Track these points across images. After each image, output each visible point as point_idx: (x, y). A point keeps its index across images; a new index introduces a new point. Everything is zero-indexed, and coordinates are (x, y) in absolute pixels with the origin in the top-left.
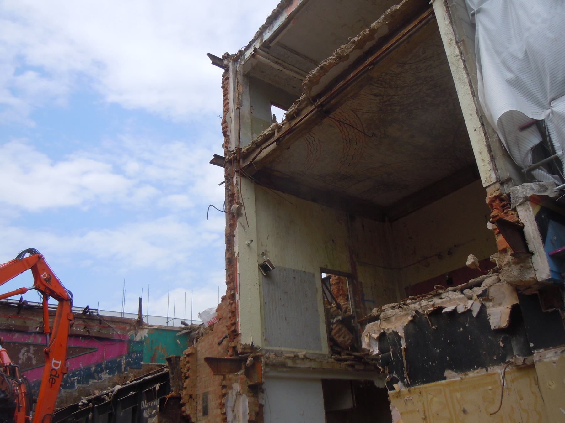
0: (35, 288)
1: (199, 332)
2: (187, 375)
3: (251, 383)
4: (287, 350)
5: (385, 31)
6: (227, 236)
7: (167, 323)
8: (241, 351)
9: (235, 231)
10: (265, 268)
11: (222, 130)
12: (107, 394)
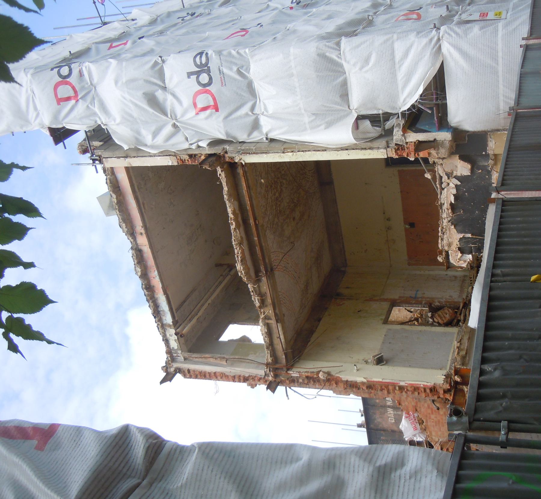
5: (236, 203)
8: (448, 385)
9: (343, 379)
10: (380, 361)
11: (240, 382)
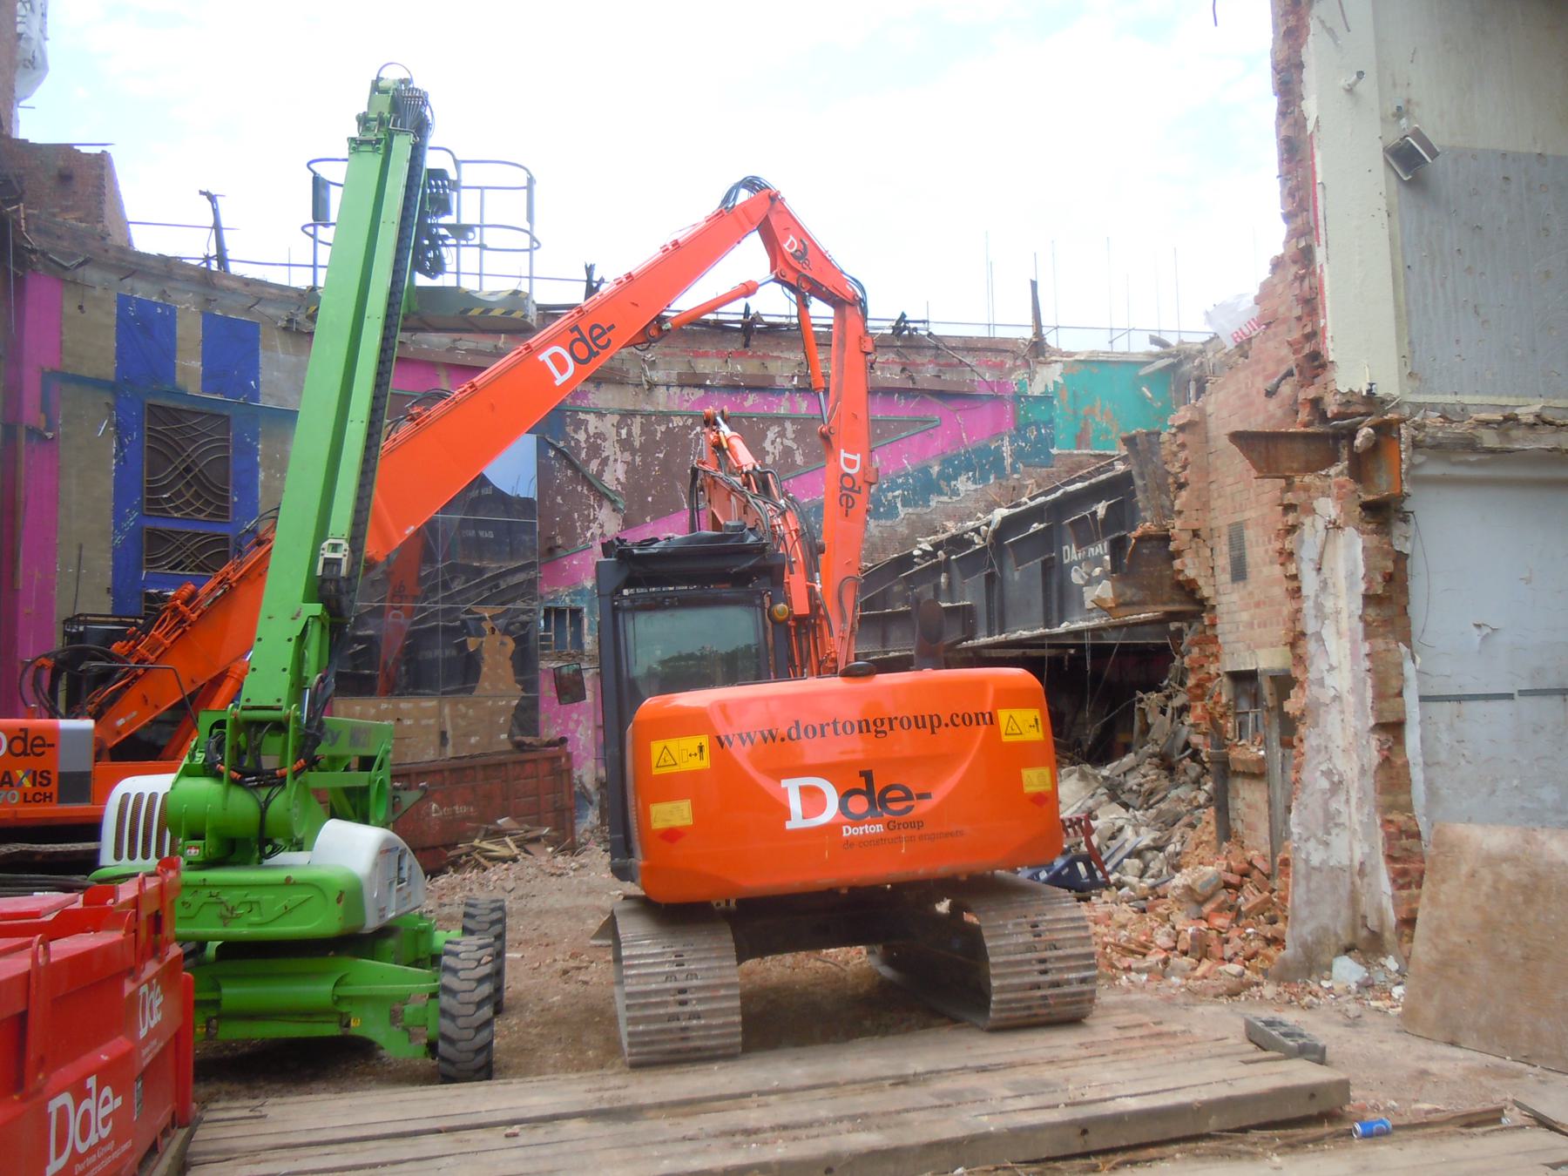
0: (777, 280)
1: (1201, 363)
2: (1182, 480)
3: (1371, 498)
4: (1483, 402)
6: (1279, 68)
7: (1111, 342)
8: (1336, 411)
9: (1304, 50)
12: (977, 530)
